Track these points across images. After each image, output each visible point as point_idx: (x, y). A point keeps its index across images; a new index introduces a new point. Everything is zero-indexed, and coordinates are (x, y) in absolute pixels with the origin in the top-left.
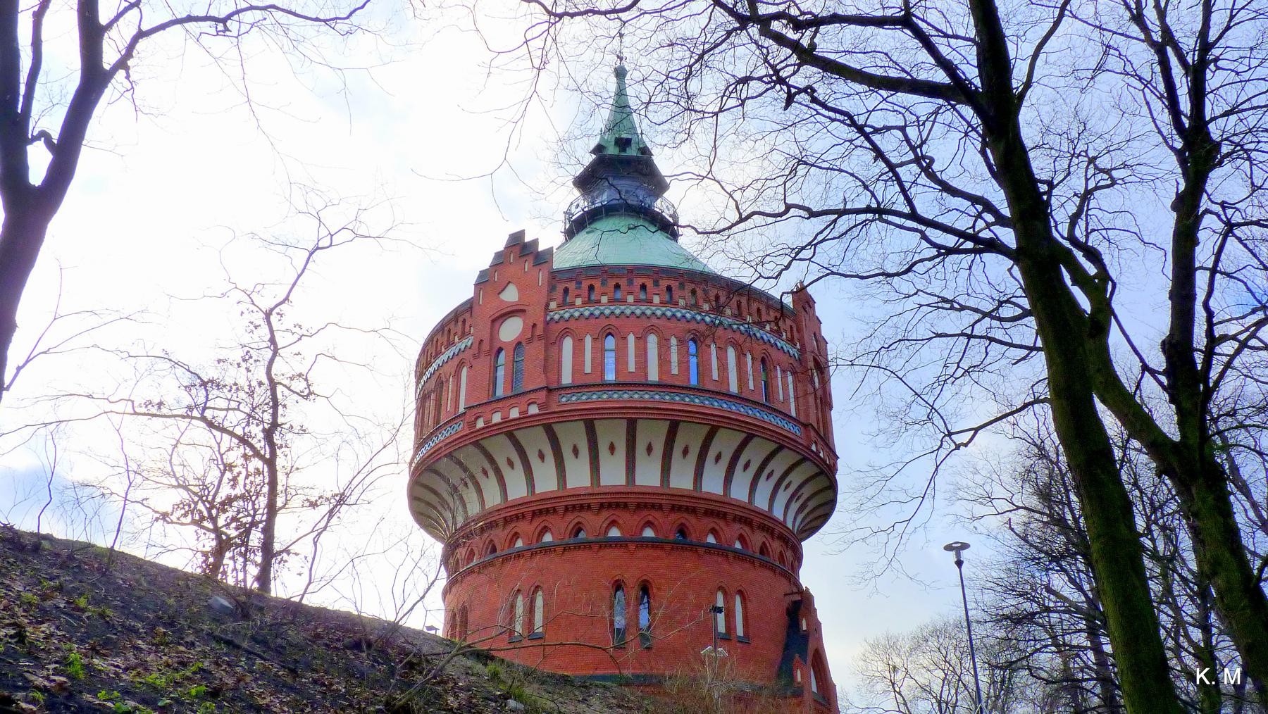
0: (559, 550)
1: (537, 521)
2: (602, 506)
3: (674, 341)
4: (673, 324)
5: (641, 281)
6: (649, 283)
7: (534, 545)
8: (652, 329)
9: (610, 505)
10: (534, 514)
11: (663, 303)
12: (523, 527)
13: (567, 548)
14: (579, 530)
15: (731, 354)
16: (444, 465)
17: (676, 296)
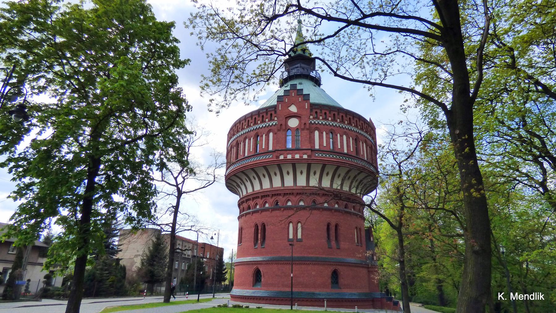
0: (270, 210)
1: (263, 199)
2: (310, 194)
3: (324, 133)
4: (326, 126)
5: (315, 110)
6: (319, 111)
7: (262, 208)
8: (317, 129)
9: (313, 194)
10: (262, 197)
11: (323, 119)
12: (260, 201)
13: (273, 210)
14: (277, 203)
15: (345, 137)
16: (235, 178)
17: (336, 118)
